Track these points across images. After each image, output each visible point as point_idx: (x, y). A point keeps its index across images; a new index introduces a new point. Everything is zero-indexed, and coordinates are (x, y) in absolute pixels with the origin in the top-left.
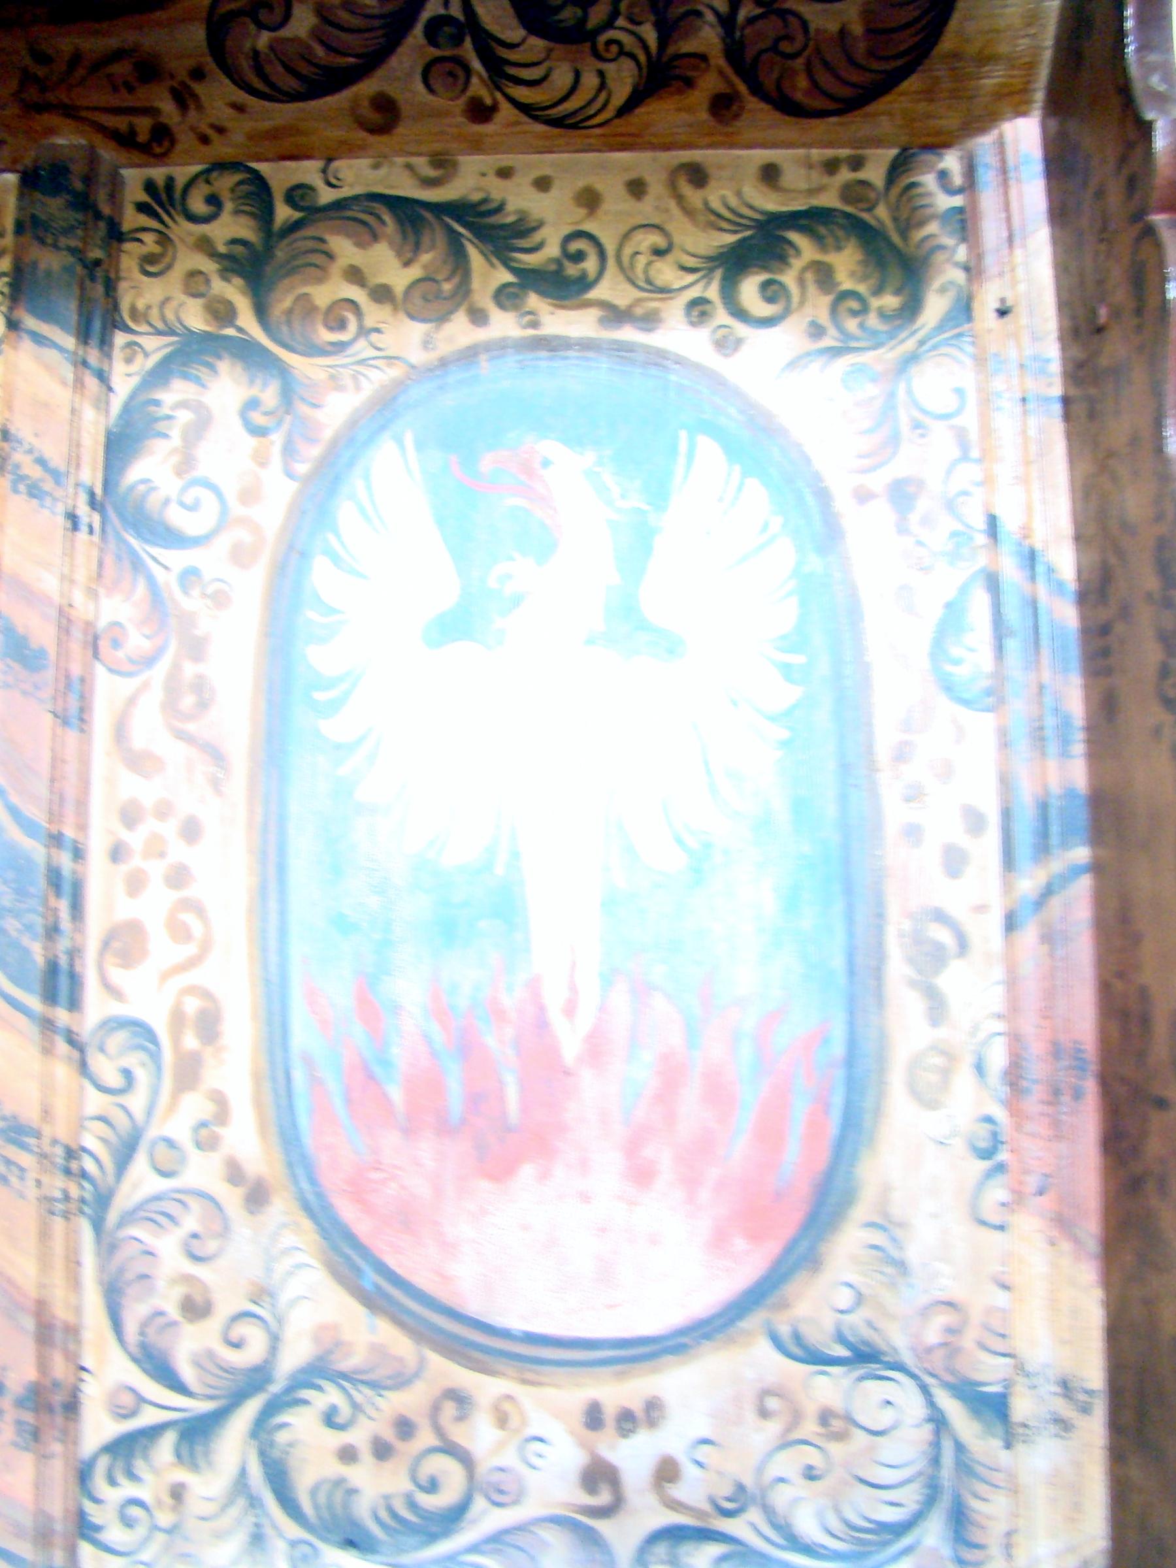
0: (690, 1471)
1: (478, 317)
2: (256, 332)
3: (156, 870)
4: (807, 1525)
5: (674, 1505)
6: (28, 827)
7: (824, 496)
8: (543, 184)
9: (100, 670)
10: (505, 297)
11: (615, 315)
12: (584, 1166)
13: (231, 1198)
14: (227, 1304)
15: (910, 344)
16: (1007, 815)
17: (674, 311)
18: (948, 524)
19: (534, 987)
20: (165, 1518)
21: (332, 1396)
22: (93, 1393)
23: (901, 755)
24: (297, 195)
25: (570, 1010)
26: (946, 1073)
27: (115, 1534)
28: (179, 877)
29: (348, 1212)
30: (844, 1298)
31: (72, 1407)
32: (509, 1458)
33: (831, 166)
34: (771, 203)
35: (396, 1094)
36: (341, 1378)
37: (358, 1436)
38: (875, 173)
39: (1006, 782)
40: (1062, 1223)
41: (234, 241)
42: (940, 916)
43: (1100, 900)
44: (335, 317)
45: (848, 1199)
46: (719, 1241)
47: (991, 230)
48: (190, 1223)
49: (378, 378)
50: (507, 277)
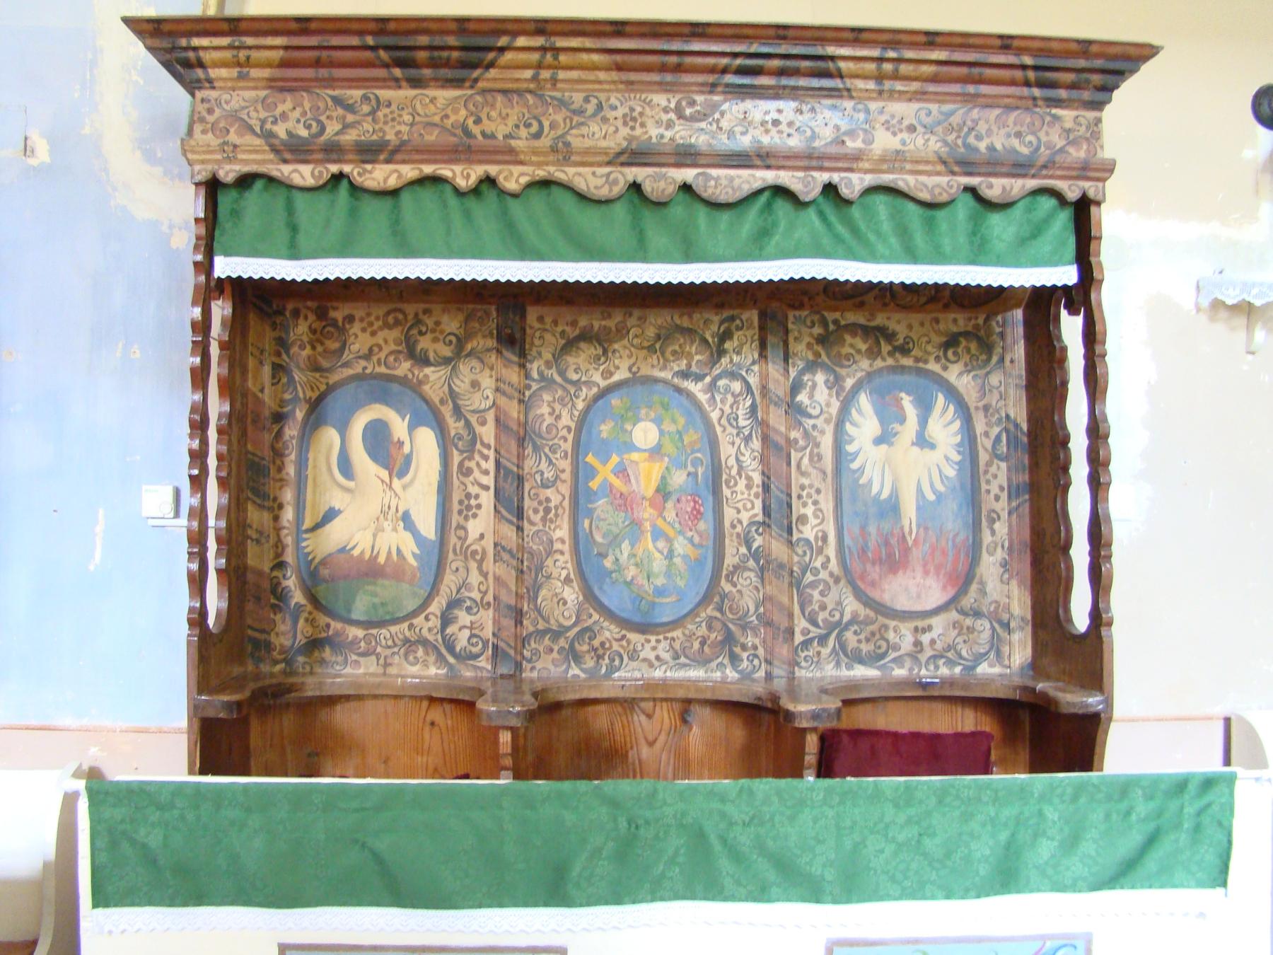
0: (938, 642)
1: (884, 359)
3: (810, 501)
4: (964, 653)
5: (935, 650)
6: (782, 492)
7: (968, 409)
8: (899, 322)
9: (792, 451)
10: (891, 354)
11: (917, 360)
12: (914, 571)
13: (831, 581)
14: (830, 607)
15: (988, 369)
16: (1009, 487)
17: (932, 359)
18: (997, 416)
19: (902, 528)
21: (856, 627)
22: (797, 630)
23: (986, 472)
24: (836, 322)
27: (803, 664)
28: (815, 503)
29: (859, 583)
30: (973, 600)
31: (793, 633)
32: (897, 640)
33: (970, 319)
34: (955, 329)
35: (870, 555)
36: (858, 623)
37: (862, 637)
38: (981, 321)
39: (1009, 479)
40: (1020, 583)
41: (820, 335)
42: (994, 511)
43: (1032, 507)
44: (848, 357)
45: (973, 577)
46: (944, 588)
47: (1009, 340)
48: (821, 587)
49: (859, 375)
50: (890, 348)
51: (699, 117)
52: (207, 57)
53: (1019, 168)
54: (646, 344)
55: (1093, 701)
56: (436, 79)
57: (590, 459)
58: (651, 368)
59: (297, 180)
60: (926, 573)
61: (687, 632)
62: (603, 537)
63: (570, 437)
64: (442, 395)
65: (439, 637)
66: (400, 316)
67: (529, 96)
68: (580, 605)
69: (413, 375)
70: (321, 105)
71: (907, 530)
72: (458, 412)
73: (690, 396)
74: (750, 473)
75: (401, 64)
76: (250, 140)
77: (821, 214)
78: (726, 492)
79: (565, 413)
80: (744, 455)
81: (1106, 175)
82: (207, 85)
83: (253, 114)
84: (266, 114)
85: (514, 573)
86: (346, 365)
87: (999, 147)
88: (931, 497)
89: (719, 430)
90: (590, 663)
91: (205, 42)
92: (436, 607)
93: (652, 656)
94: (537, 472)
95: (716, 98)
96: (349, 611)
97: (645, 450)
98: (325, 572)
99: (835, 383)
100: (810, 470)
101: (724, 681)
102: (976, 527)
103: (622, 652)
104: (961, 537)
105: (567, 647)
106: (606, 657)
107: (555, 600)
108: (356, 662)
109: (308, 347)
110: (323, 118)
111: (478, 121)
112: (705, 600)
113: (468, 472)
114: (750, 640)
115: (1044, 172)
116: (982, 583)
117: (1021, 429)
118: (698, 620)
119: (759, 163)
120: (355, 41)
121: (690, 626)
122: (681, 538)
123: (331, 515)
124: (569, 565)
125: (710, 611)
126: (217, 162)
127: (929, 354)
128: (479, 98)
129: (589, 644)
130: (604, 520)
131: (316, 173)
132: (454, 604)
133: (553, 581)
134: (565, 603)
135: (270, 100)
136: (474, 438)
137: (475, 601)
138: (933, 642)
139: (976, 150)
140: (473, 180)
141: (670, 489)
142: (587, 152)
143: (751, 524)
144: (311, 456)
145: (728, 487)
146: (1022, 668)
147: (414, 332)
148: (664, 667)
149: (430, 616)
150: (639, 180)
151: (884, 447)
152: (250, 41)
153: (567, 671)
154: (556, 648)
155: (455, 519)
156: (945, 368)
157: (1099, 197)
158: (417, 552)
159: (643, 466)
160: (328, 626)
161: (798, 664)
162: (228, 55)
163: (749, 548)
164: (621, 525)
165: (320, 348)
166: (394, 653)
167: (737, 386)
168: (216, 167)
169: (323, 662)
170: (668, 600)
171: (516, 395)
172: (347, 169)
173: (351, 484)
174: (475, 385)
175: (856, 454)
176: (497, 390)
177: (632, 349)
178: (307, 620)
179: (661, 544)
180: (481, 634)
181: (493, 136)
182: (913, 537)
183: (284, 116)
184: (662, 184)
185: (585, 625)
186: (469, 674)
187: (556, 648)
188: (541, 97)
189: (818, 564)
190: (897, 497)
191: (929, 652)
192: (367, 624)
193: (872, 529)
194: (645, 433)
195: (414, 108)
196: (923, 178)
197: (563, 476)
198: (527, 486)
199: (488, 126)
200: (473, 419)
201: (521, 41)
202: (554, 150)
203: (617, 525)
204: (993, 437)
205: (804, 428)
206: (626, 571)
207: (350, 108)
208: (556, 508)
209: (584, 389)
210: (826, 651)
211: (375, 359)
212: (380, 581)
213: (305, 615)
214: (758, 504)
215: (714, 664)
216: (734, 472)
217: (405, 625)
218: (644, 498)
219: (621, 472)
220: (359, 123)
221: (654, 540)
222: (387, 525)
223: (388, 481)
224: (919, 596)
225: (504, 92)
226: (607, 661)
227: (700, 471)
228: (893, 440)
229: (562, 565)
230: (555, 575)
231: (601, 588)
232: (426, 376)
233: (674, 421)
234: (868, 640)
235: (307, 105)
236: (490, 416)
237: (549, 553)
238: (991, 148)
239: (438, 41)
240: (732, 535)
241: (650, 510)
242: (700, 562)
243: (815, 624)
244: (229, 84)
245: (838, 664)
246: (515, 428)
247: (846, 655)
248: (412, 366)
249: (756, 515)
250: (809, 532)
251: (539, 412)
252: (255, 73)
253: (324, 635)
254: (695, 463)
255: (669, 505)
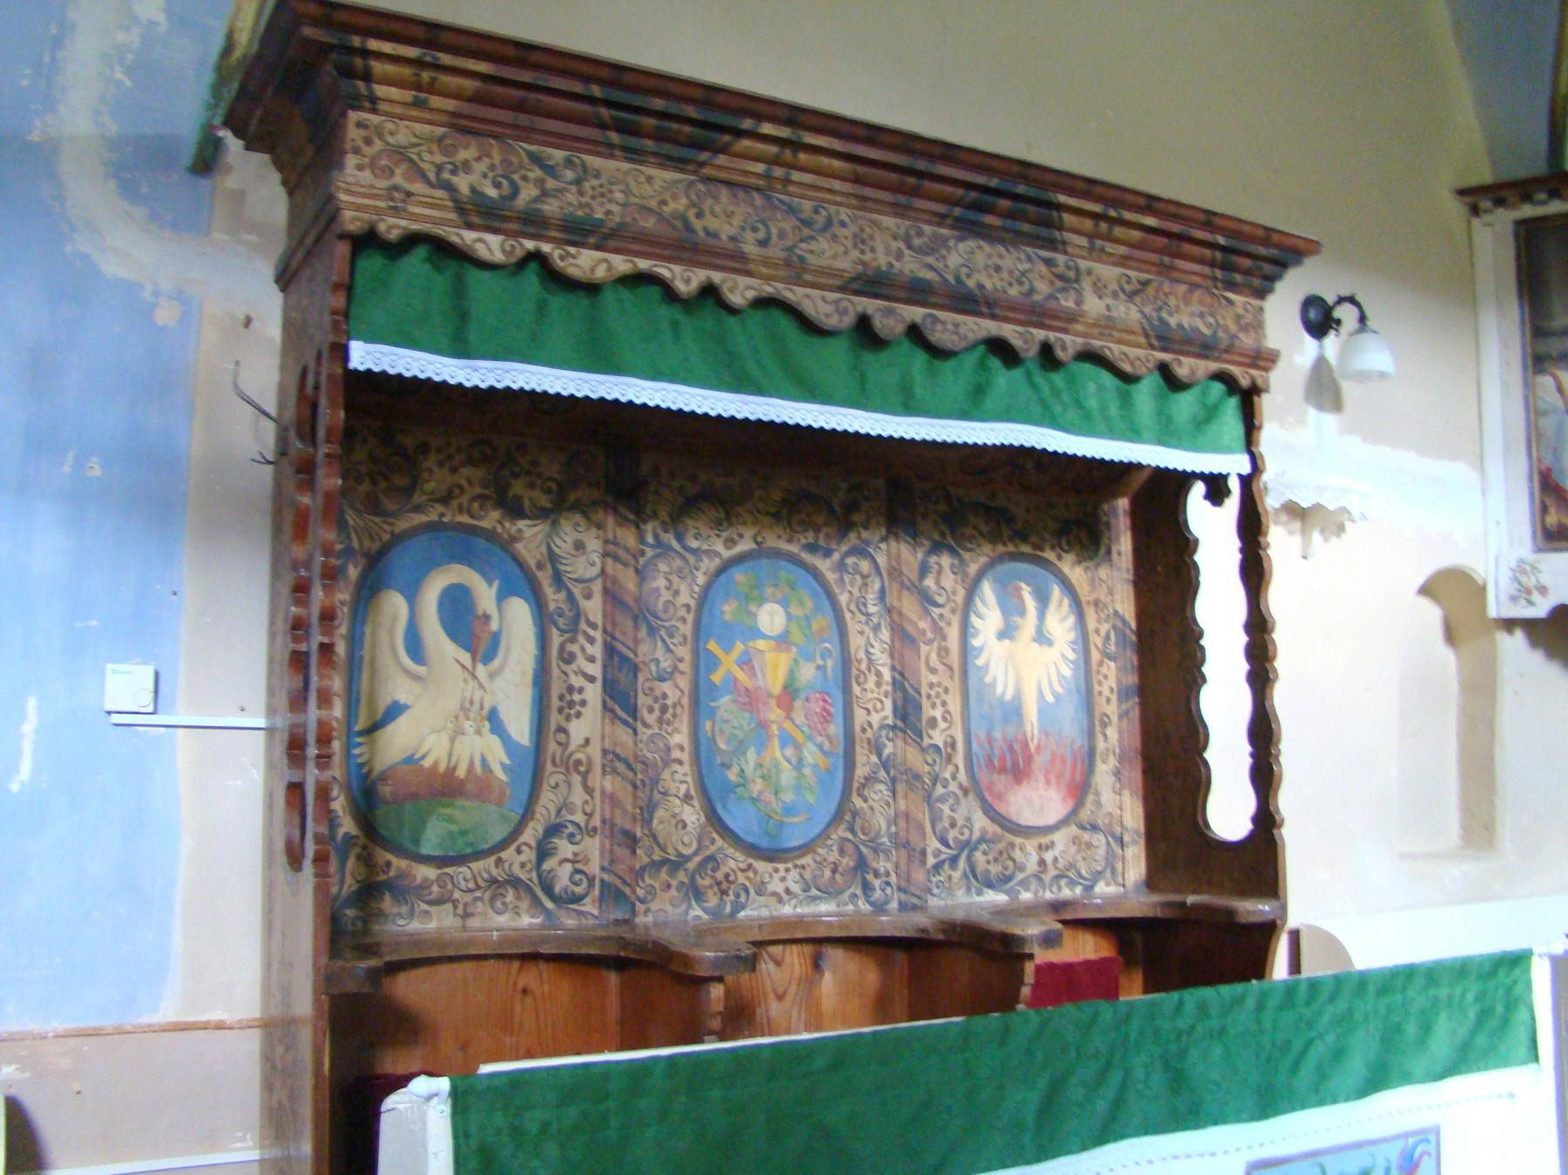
1: (1005, 544)
2: (952, 543)
4: (1084, 872)
10: (1011, 539)
12: (1036, 780)
13: (959, 793)
20: (947, 885)
21: (984, 846)
22: (929, 851)
24: (959, 499)
25: (1032, 740)
26: (1107, 755)
27: (936, 891)
28: (944, 704)
34: (1066, 515)
35: (996, 762)
37: (990, 857)
45: (1089, 785)
48: (951, 801)
51: (927, 250)
52: (378, 67)
53: (1205, 349)
54: (772, 510)
55: (1255, 909)
56: (656, 154)
57: (712, 646)
58: (775, 540)
59: (482, 252)
60: (1048, 782)
61: (818, 858)
62: (727, 742)
63: (690, 618)
64: (539, 556)
65: (534, 876)
66: (488, 450)
67: (755, 195)
68: (702, 827)
69: (503, 527)
70: (514, 160)
71: (1029, 735)
72: (558, 579)
73: (815, 573)
74: (880, 668)
75: (621, 128)
76: (418, 187)
77: (1029, 375)
78: (856, 689)
79: (683, 588)
80: (872, 646)
81: (1269, 364)
82: (367, 105)
83: (426, 156)
84: (445, 159)
85: (630, 788)
86: (418, 509)
87: (1186, 325)
88: (1050, 699)
89: (848, 615)
90: (712, 900)
91: (387, 47)
92: (530, 835)
93: (780, 888)
94: (651, 661)
95: (944, 232)
96: (417, 842)
97: (771, 638)
98: (385, 790)
99: (957, 570)
100: (940, 667)
101: (857, 913)
102: (1091, 734)
103: (748, 884)
104: (1078, 744)
105: (686, 881)
106: (731, 892)
107: (674, 822)
108: (427, 912)
109: (367, 480)
110: (516, 177)
111: (700, 215)
112: (837, 818)
113: (569, 659)
114: (882, 865)
115: (1225, 356)
116: (1097, 794)
117: (1130, 626)
118: (829, 842)
119: (985, 310)
120: (577, 87)
121: (820, 851)
122: (810, 746)
123: (395, 711)
124: (689, 779)
125: (842, 832)
126: (378, 211)
127: (1044, 540)
128: (701, 187)
129: (712, 877)
130: (727, 721)
131: (508, 248)
132: (553, 830)
133: (669, 798)
134: (685, 826)
135: (448, 141)
136: (578, 615)
137: (577, 825)
138: (1056, 860)
139: (1167, 324)
140: (694, 285)
141: (798, 685)
142: (820, 271)
143: (882, 727)
144: (368, 630)
145: (859, 684)
146: (1136, 886)
147: (505, 472)
148: (793, 902)
149: (524, 848)
150: (870, 311)
151: (1007, 642)
152: (446, 59)
153: (687, 913)
154: (674, 883)
155: (555, 719)
156: (1059, 558)
157: (1265, 387)
158: (508, 762)
159: (770, 657)
160: (389, 864)
161: (929, 891)
162: (406, 72)
163: (879, 755)
164: (746, 728)
165: (383, 484)
166: (476, 899)
167: (865, 566)
168: (375, 217)
169: (381, 914)
170: (796, 819)
171: (633, 562)
172: (546, 248)
173: (422, 670)
174: (580, 546)
175: (981, 649)
176: (605, 555)
177: (758, 515)
178: (359, 857)
179: (789, 752)
180: (585, 869)
181: (715, 236)
182: (1036, 741)
183: (466, 166)
184: (891, 322)
185: (708, 853)
186: (570, 922)
187: (674, 883)
188: (768, 198)
189: (947, 775)
190: (1020, 699)
191: (1052, 872)
192: (440, 861)
193: (997, 735)
194: (771, 618)
195: (627, 186)
196: (1125, 348)
197: (682, 666)
198: (641, 678)
199: (712, 223)
200: (577, 591)
201: (767, 128)
202: (788, 264)
203: (741, 728)
204: (1103, 633)
205: (932, 618)
206: (752, 785)
207: (550, 170)
208: (674, 706)
209: (706, 560)
210: (956, 875)
211: (455, 503)
212: (460, 802)
213: (357, 850)
214: (888, 703)
215: (846, 896)
216: (864, 666)
217: (491, 860)
218: (770, 695)
219: (746, 663)
220: (559, 191)
221: (783, 747)
222: (469, 726)
223: (470, 669)
224: (1042, 809)
225: (729, 184)
226: (732, 897)
227: (830, 663)
228: (1015, 634)
229: (679, 779)
230: (673, 791)
231: (724, 807)
232: (520, 531)
233: (801, 603)
234: (996, 860)
235: (497, 158)
236: (597, 587)
237: (667, 763)
238: (1180, 326)
239: (674, 108)
240: (862, 742)
241: (779, 711)
242: (830, 771)
243: (946, 844)
244: (398, 110)
245: (968, 889)
246: (631, 603)
247: (975, 876)
248: (503, 516)
249: (886, 717)
250: (938, 738)
251: (654, 585)
252: (436, 101)
253: (383, 877)
254: (825, 654)
255: (798, 704)
